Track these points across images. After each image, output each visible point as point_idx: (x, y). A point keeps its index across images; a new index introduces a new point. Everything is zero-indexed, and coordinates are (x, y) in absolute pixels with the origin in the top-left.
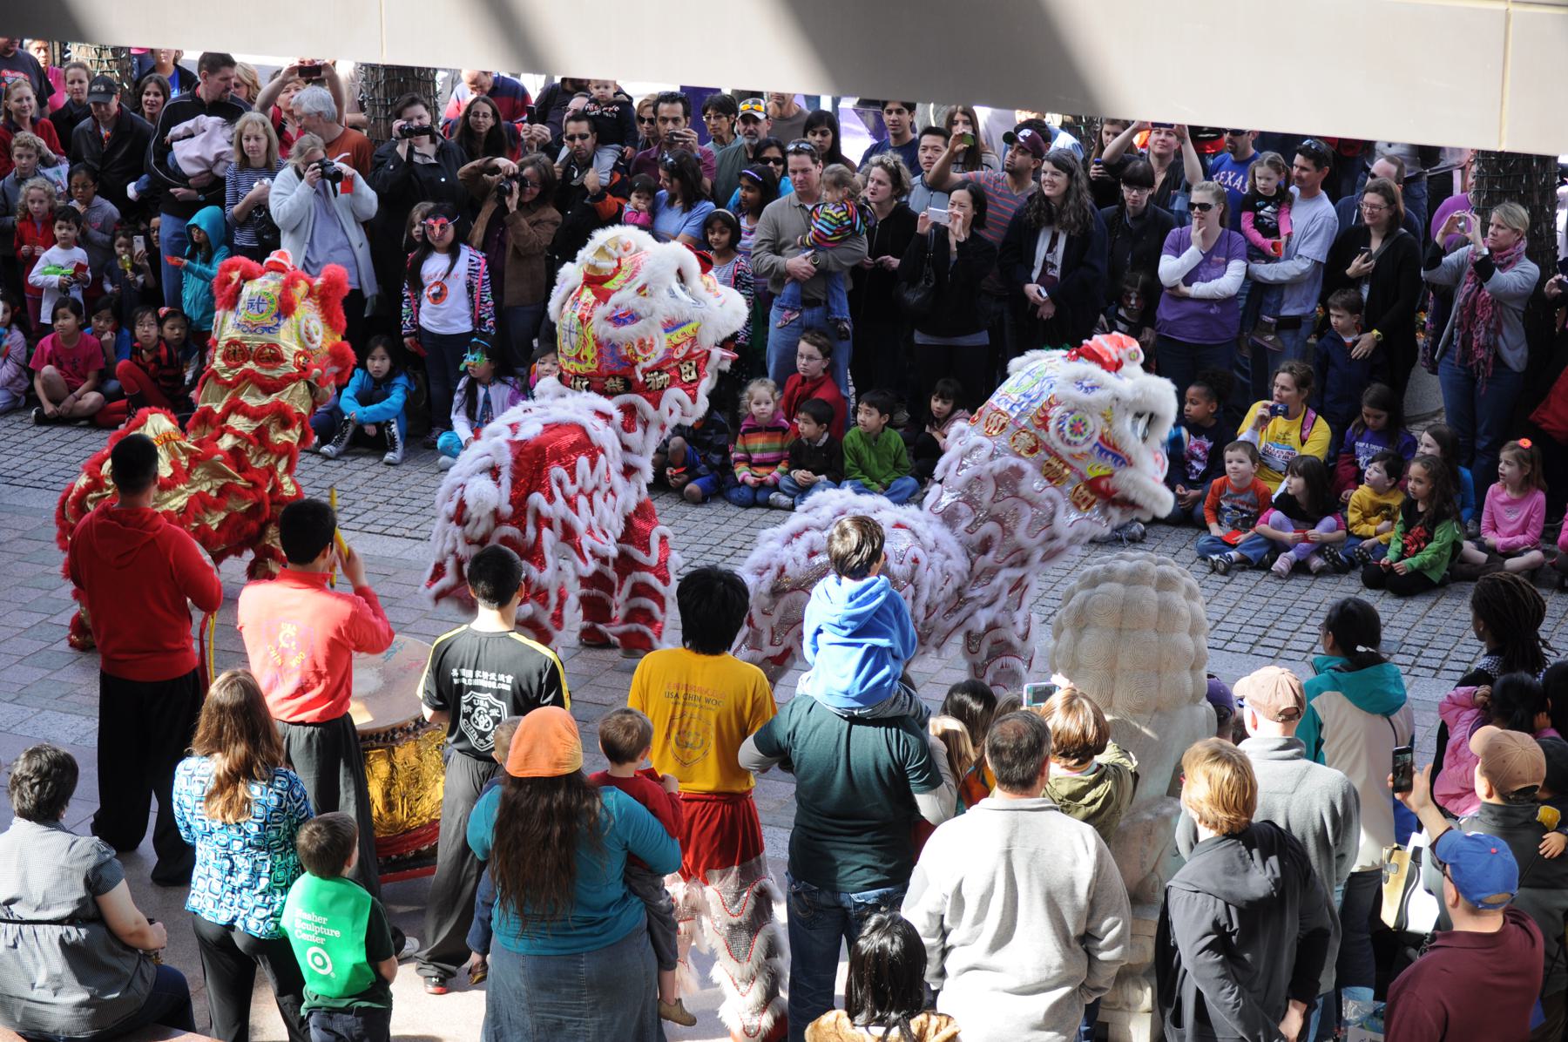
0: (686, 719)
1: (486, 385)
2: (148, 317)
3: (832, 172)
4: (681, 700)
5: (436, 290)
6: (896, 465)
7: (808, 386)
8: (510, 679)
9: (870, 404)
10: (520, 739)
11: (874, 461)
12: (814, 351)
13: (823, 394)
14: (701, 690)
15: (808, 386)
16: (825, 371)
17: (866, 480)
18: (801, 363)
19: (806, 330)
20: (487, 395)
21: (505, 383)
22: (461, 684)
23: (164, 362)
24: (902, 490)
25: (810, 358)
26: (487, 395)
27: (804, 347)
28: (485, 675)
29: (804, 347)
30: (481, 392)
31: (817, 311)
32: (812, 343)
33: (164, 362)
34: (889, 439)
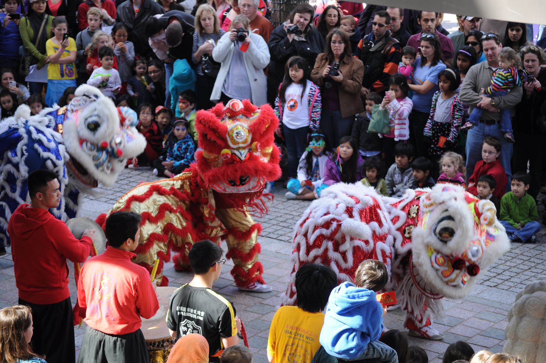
0: (295, 347)
1: (318, 156)
2: (148, 109)
3: (506, 51)
4: (293, 336)
5: (292, 103)
6: (530, 215)
7: (486, 166)
8: (203, 314)
9: (519, 180)
10: (175, 351)
11: (517, 211)
12: (492, 148)
13: (493, 172)
14: (304, 331)
15: (486, 166)
16: (497, 159)
17: (511, 221)
18: (485, 155)
19: (486, 137)
20: (317, 162)
21: (327, 155)
22: (180, 315)
23: (156, 133)
24: (531, 229)
25: (490, 152)
26: (317, 162)
27: (486, 146)
28: (192, 310)
29: (486, 146)
30: (315, 160)
31: (493, 127)
32: (490, 144)
33: (156, 133)
34: (527, 200)
